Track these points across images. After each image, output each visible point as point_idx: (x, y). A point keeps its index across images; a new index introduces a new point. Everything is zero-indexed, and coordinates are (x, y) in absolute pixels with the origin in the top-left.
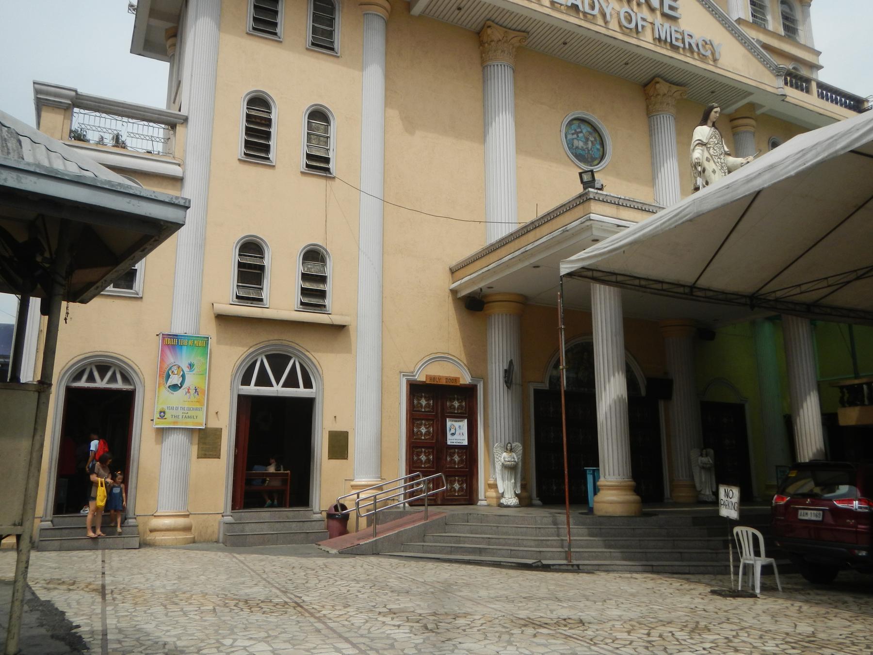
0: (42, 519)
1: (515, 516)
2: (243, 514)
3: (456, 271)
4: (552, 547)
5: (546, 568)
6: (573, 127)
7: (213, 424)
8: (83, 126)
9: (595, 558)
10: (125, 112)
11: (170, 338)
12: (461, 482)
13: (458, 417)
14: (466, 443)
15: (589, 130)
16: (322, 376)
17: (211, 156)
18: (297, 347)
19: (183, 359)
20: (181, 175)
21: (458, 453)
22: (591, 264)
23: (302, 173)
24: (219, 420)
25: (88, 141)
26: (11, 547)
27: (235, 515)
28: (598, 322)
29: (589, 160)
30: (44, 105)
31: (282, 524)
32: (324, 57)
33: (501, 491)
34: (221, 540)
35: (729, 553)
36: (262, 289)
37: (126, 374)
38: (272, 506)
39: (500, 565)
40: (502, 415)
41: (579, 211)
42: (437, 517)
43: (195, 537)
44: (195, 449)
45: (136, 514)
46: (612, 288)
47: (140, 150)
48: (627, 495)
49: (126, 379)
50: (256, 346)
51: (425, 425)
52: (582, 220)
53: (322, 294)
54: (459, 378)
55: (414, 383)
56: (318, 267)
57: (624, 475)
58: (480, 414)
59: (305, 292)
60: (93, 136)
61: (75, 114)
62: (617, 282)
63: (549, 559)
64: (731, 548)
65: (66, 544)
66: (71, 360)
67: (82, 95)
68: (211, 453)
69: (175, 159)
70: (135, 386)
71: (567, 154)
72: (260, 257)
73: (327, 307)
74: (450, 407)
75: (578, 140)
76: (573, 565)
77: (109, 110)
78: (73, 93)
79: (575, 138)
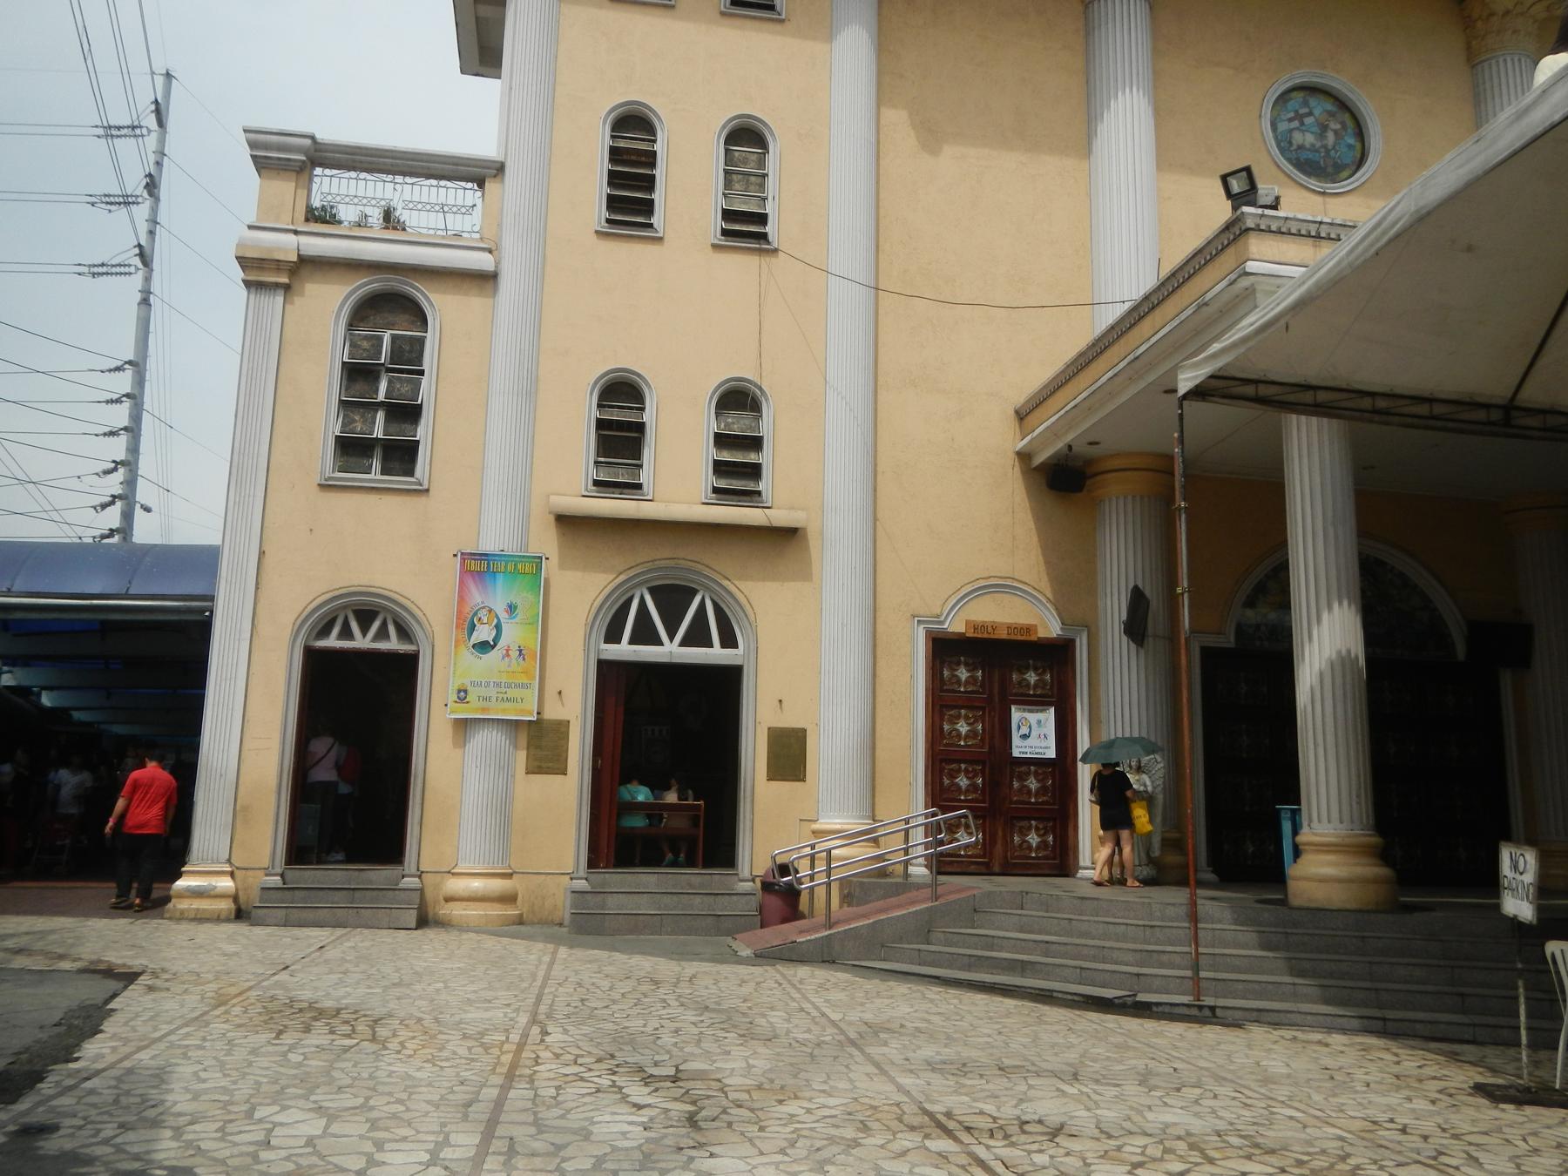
0: (267, 872)
1: (1111, 901)
2: (607, 875)
4: (1172, 966)
5: (1142, 1010)
6: (1291, 105)
7: (553, 713)
8: (329, 198)
9: (1260, 995)
10: (397, 165)
12: (1042, 832)
13: (1035, 702)
14: (1051, 754)
15: (1329, 106)
18: (707, 572)
19: (498, 596)
20: (492, 268)
21: (1036, 774)
22: (1227, 365)
23: (714, 246)
24: (563, 705)
25: (340, 222)
26: (216, 917)
27: (592, 877)
28: (1294, 496)
29: (1330, 170)
30: (264, 168)
31: (675, 898)
32: (757, 24)
34: (566, 922)
35: (1516, 998)
36: (641, 466)
37: (401, 623)
38: (674, 864)
39: (1052, 997)
41: (1227, 260)
42: (957, 896)
43: (521, 915)
44: (521, 756)
45: (421, 869)
46: (1325, 420)
47: (424, 231)
48: (1375, 865)
49: (404, 633)
50: (629, 572)
51: (967, 718)
52: (1233, 276)
53: (754, 471)
54: (1036, 626)
56: (747, 422)
57: (1352, 822)
59: (723, 468)
60: (347, 214)
61: (315, 179)
62: (1317, 405)
63: (1156, 992)
64: (1521, 990)
65: (295, 914)
66: (311, 602)
67: (324, 144)
70: (418, 646)
71: (1276, 163)
72: (638, 409)
73: (764, 494)
74: (1019, 683)
75: (1303, 131)
76: (1201, 1008)
77: (374, 166)
78: (308, 142)
79: (1297, 129)
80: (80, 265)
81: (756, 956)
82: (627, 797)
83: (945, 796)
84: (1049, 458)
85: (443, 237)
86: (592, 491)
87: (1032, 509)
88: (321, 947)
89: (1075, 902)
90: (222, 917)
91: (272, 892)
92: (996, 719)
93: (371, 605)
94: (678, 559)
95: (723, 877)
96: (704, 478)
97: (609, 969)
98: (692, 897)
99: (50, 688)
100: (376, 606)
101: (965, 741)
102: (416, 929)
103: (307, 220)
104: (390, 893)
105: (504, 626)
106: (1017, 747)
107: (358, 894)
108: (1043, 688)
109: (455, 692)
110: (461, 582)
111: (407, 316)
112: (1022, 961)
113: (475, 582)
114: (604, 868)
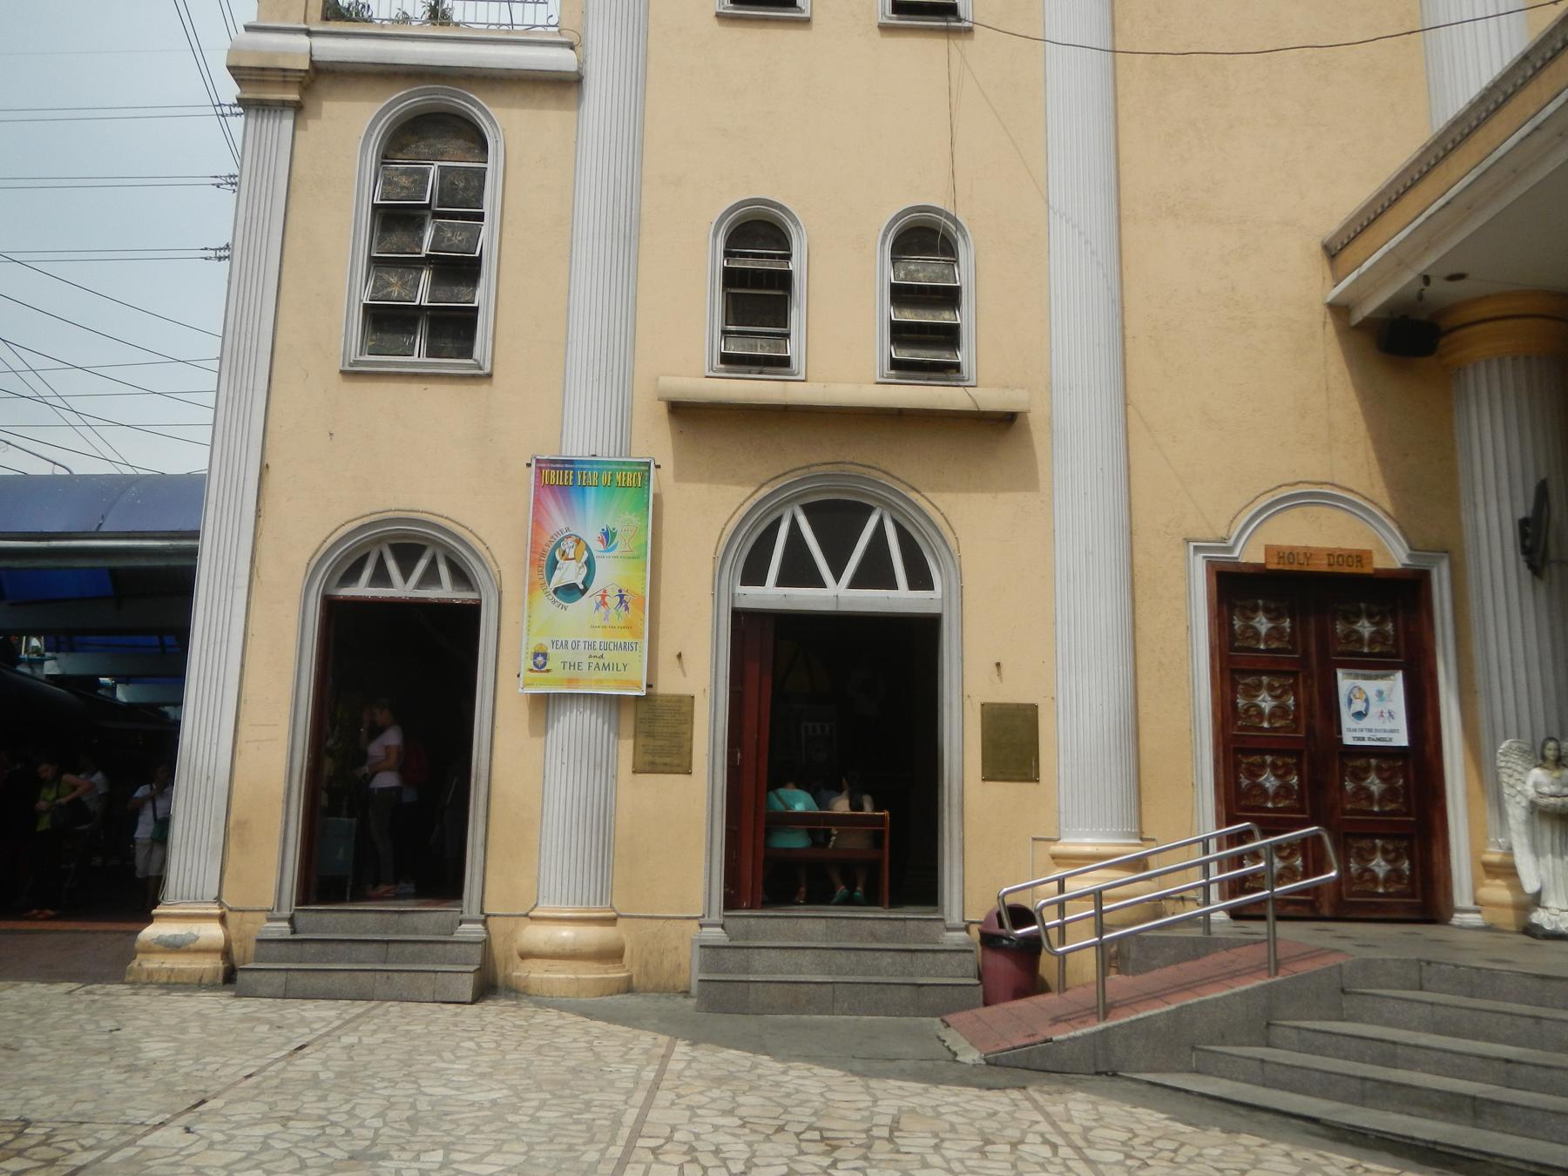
2: (752, 921)
3: (1344, 247)
7: (670, 684)
11: (555, 469)
12: (1392, 856)
13: (1373, 663)
14: (1401, 739)
16: (956, 555)
17: (647, 14)
18: (884, 480)
20: (574, 68)
21: (1379, 771)
23: (884, 28)
25: (369, 20)
27: (729, 923)
31: (852, 955)
33: (1531, 886)
34: (694, 991)
36: (787, 336)
38: (849, 901)
40: (1520, 656)
43: (630, 978)
44: (626, 748)
45: (485, 911)
49: (461, 576)
51: (1271, 688)
53: (949, 336)
54: (1370, 552)
55: (1232, 569)
56: (937, 269)
58: (1445, 655)
65: (300, 981)
66: (332, 534)
68: (667, 760)
69: (561, 35)
70: (480, 593)
73: (964, 368)
74: (1347, 636)
80: (206, 249)
81: (988, 1063)
82: (779, 807)
83: (1243, 803)
84: (1375, 311)
85: (508, 32)
86: (719, 370)
87: (1355, 385)
88: (301, 1048)
89: (1528, 983)
90: (205, 980)
91: (273, 945)
92: (1315, 690)
93: (415, 537)
94: (844, 463)
95: (922, 924)
96: (878, 348)
97: (750, 1103)
98: (878, 954)
99: (125, 679)
100: (422, 538)
101: (1270, 722)
102: (472, 1003)
103: (326, 18)
104: (440, 946)
105: (598, 562)
106: (1349, 730)
107: (393, 949)
108: (1383, 644)
109: (531, 656)
110: (537, 501)
111: (461, 142)
112: (1474, 1098)
113: (556, 500)
114: (747, 908)
